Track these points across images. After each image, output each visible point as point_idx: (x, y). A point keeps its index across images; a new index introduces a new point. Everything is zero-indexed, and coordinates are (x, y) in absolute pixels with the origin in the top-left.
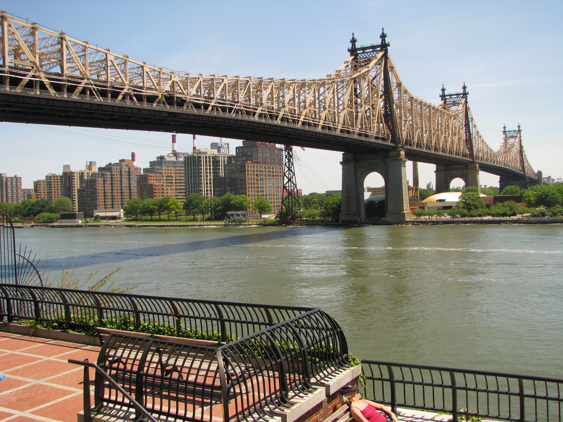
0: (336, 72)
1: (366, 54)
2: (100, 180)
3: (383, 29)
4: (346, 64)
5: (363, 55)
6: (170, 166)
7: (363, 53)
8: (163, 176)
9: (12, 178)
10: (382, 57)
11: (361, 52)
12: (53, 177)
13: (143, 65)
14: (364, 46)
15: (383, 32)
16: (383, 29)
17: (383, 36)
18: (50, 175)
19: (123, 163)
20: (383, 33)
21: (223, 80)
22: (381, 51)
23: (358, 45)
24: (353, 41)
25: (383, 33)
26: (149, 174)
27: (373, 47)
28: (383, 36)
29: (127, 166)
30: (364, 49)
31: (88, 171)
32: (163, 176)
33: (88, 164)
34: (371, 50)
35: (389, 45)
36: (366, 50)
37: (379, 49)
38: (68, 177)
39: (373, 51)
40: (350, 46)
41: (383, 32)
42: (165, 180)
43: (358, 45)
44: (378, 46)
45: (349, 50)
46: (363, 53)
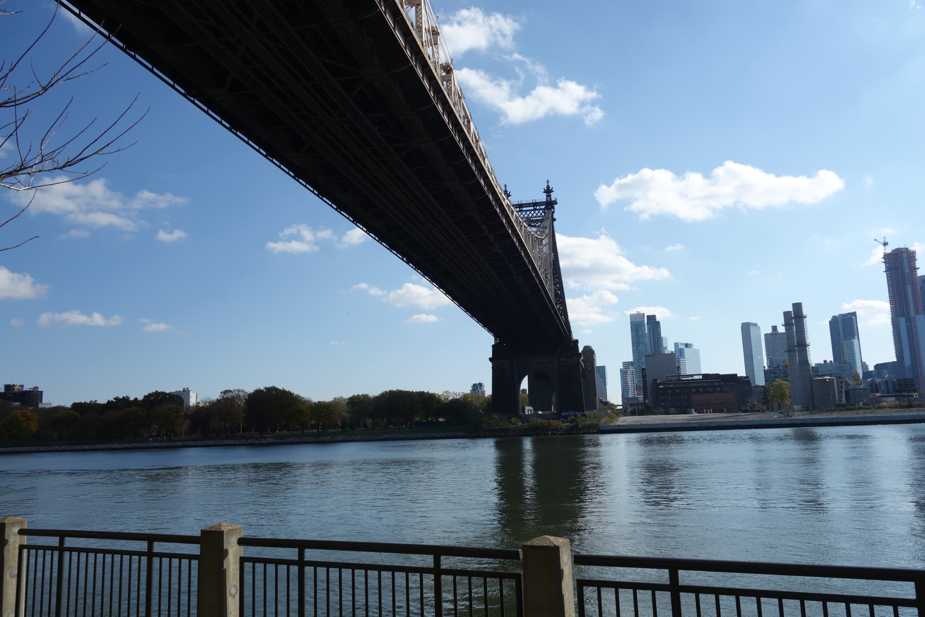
1: (524, 213)
5: (520, 213)
14: (522, 203)
15: (548, 185)
17: (548, 191)
20: (548, 187)
25: (548, 187)
27: (535, 204)
28: (548, 191)
30: (520, 206)
34: (532, 208)
35: (556, 203)
37: (543, 207)
39: (535, 209)
41: (548, 185)
46: (520, 211)
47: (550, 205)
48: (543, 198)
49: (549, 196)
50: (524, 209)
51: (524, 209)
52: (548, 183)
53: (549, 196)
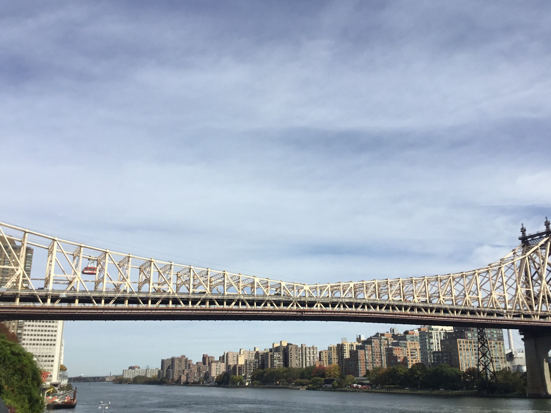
0: (501, 260)
2: (361, 353)
4: (513, 252)
6: (414, 341)
7: (532, 240)
8: (407, 349)
9: (309, 348)
10: (546, 242)
11: (529, 239)
12: (332, 348)
13: (280, 282)
14: (532, 234)
18: (331, 346)
19: (383, 337)
21: (349, 284)
22: (546, 237)
23: (527, 234)
24: (523, 230)
26: (394, 347)
27: (540, 235)
29: (386, 339)
31: (357, 343)
32: (407, 349)
33: (358, 337)
34: (538, 237)
36: (536, 236)
37: (545, 235)
38: (340, 348)
40: (520, 235)
42: (409, 352)
43: (527, 234)
44: (543, 233)
45: (520, 239)
50: (535, 238)
51: (535, 238)
52: (546, 218)
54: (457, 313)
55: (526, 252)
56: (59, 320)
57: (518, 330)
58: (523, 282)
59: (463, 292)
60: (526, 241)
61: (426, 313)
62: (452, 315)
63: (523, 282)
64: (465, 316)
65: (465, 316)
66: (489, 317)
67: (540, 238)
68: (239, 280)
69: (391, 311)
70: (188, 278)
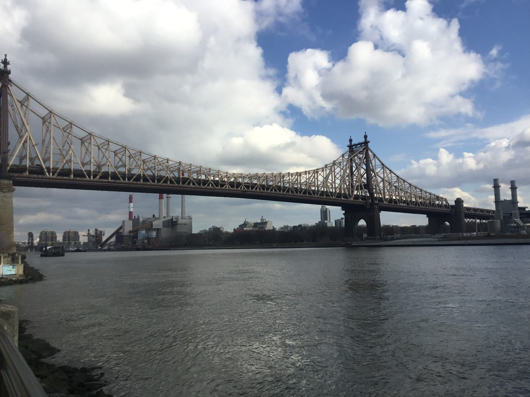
3: (365, 133)
10: (364, 149)
16: (365, 133)
17: (366, 137)
27: (360, 144)
28: (366, 137)
34: (359, 146)
37: (363, 145)
44: (362, 143)
47: (366, 143)
48: (363, 140)
49: (366, 139)
53: (366, 139)
54: (317, 195)
55: (351, 156)
56: (380, 224)
57: (340, 207)
58: (346, 176)
59: (293, 178)
60: (351, 147)
61: (314, 196)
62: (314, 196)
63: (346, 176)
64: (323, 197)
65: (323, 197)
66: (337, 199)
67: (360, 146)
68: (190, 169)
69: (266, 191)
70: (153, 165)
